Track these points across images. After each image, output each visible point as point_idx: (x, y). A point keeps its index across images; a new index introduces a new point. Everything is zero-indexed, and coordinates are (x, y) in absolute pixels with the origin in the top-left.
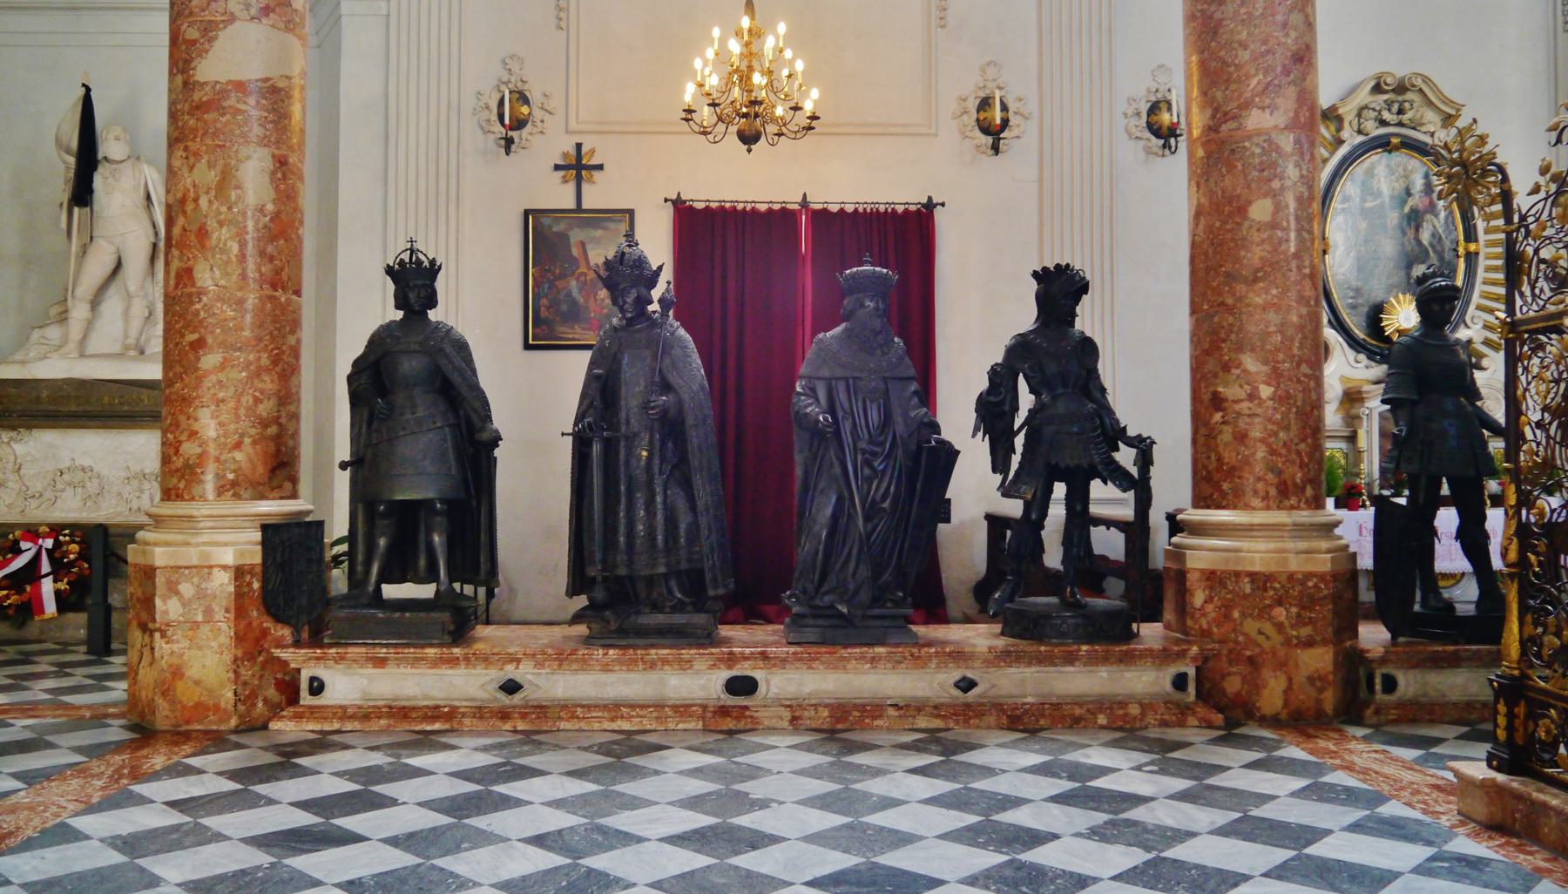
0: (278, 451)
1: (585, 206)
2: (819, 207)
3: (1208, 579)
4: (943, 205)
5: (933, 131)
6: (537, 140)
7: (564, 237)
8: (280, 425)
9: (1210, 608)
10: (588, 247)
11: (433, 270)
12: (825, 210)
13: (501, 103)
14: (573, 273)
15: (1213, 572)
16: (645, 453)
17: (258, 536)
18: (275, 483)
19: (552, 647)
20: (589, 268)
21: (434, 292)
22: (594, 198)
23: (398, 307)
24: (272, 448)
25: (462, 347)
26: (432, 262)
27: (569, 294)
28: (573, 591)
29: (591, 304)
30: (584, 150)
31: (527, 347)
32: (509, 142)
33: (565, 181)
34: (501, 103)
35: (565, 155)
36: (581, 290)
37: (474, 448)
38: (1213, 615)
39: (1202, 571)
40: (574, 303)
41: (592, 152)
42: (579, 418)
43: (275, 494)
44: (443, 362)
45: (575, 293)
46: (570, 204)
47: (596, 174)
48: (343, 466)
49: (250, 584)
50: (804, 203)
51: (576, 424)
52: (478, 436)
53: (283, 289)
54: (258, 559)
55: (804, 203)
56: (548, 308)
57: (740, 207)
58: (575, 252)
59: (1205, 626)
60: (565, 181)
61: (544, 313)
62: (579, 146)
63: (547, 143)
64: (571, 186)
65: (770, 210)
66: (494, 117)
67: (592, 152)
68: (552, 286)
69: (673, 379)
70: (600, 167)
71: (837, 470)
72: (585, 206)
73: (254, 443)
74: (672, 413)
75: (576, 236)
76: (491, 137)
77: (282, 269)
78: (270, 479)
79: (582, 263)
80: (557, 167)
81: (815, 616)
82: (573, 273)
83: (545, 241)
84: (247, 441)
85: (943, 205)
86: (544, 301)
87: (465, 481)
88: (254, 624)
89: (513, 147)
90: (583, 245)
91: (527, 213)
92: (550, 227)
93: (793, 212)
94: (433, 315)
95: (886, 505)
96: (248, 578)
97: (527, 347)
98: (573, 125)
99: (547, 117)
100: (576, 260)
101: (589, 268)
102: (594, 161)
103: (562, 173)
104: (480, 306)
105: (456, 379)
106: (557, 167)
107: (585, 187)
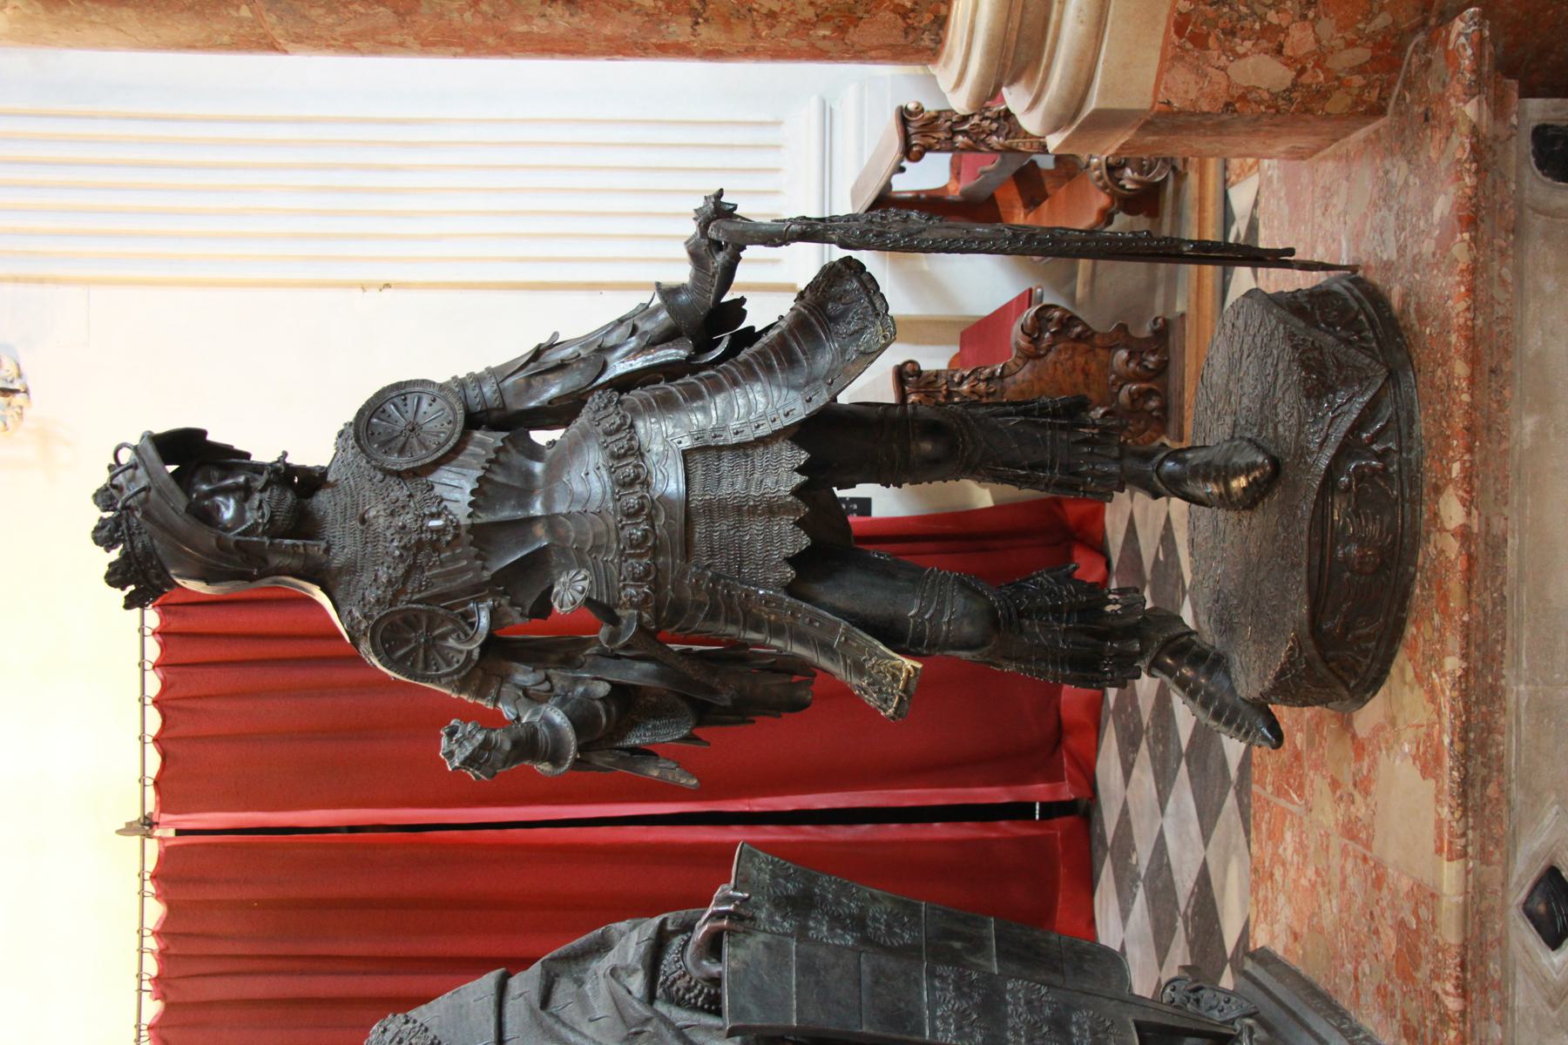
2: (151, 793)
3: (1200, 41)
9: (1300, 39)
15: (1180, 24)
38: (1327, 27)
39: (1169, 60)
55: (147, 825)
59: (1362, 54)
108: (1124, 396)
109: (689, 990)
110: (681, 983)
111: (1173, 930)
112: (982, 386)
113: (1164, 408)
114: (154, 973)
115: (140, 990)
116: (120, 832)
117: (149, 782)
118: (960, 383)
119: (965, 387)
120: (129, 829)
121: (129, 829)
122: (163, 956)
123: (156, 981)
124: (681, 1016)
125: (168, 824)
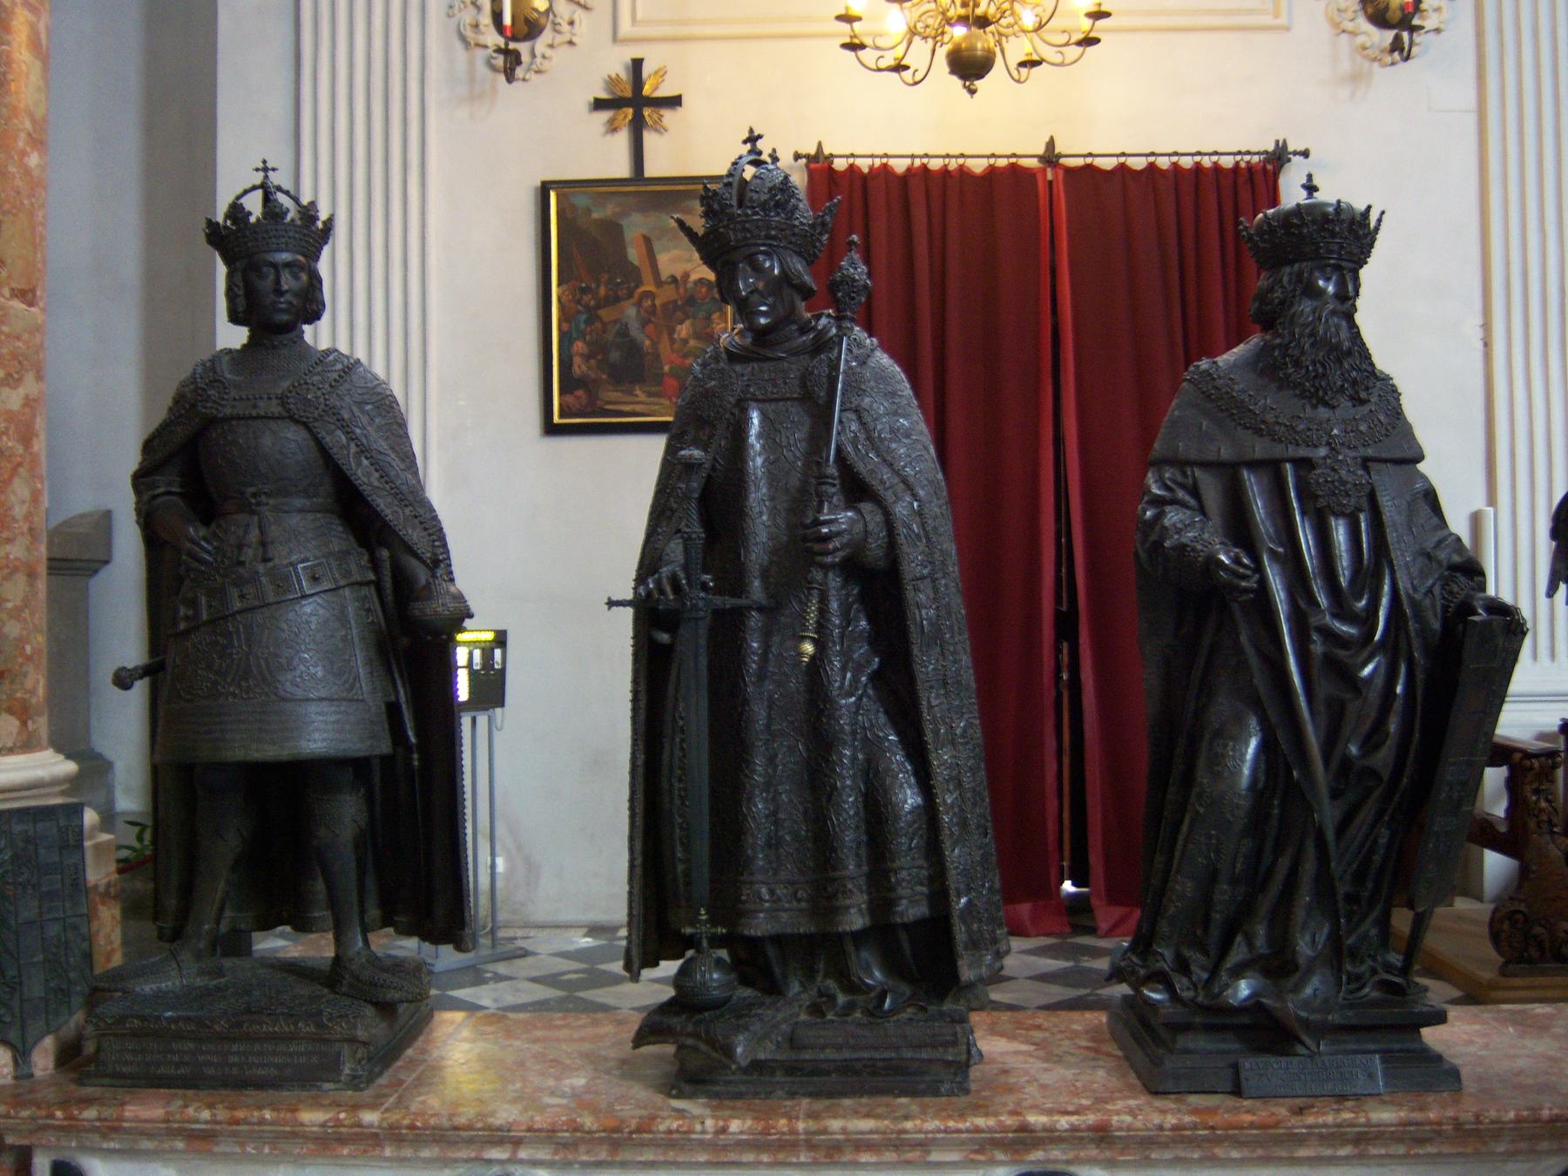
1: (651, 171)
2: (1080, 162)
4: (1306, 154)
5: (1282, 21)
6: (560, 56)
7: (613, 229)
10: (657, 246)
11: (312, 233)
12: (1089, 167)
14: (630, 296)
16: (808, 648)
19: (595, 1111)
20: (659, 283)
21: (315, 280)
22: (663, 159)
23: (235, 318)
26: (309, 213)
27: (624, 332)
28: (643, 955)
29: (665, 348)
30: (647, 70)
31: (551, 429)
32: (513, 59)
33: (612, 128)
35: (612, 82)
36: (645, 323)
37: (411, 628)
40: (633, 348)
41: (661, 73)
42: (649, 564)
44: (336, 439)
45: (635, 331)
46: (620, 167)
47: (668, 116)
48: (123, 680)
50: (1050, 157)
51: (640, 579)
52: (418, 609)
55: (1050, 157)
56: (587, 358)
57: (935, 164)
58: (634, 255)
60: (612, 128)
61: (580, 366)
62: (637, 64)
63: (580, 63)
64: (622, 139)
65: (992, 170)
66: (486, 19)
67: (661, 73)
68: (593, 317)
69: (868, 464)
70: (675, 102)
71: (1260, 681)
72: (651, 171)
74: (875, 548)
75: (635, 226)
76: (481, 55)
79: (647, 275)
80: (599, 105)
81: (1209, 1028)
82: (630, 296)
83: (584, 239)
85: (1306, 154)
86: (579, 346)
87: (393, 710)
89: (519, 72)
90: (647, 241)
91: (545, 188)
92: (589, 211)
93: (1028, 173)
94: (318, 336)
95: (1383, 758)
97: (551, 429)
98: (625, 27)
99: (579, 14)
100: (636, 271)
101: (659, 283)
102: (665, 91)
103: (605, 116)
104: (440, 324)
105: (363, 474)
106: (599, 105)
107: (649, 138)
108: (1538, 930)
109: (1451, 593)
110: (1456, 589)
111: (1075, 986)
112: (1545, 818)
113: (1530, 961)
114: (951, 168)
115: (913, 157)
116: (1052, 139)
117: (1089, 160)
118: (1547, 800)
119: (1543, 804)
120: (1051, 144)
121: (1051, 144)
122: (945, 171)
123: (924, 167)
124: (1437, 590)
125: (1056, 175)
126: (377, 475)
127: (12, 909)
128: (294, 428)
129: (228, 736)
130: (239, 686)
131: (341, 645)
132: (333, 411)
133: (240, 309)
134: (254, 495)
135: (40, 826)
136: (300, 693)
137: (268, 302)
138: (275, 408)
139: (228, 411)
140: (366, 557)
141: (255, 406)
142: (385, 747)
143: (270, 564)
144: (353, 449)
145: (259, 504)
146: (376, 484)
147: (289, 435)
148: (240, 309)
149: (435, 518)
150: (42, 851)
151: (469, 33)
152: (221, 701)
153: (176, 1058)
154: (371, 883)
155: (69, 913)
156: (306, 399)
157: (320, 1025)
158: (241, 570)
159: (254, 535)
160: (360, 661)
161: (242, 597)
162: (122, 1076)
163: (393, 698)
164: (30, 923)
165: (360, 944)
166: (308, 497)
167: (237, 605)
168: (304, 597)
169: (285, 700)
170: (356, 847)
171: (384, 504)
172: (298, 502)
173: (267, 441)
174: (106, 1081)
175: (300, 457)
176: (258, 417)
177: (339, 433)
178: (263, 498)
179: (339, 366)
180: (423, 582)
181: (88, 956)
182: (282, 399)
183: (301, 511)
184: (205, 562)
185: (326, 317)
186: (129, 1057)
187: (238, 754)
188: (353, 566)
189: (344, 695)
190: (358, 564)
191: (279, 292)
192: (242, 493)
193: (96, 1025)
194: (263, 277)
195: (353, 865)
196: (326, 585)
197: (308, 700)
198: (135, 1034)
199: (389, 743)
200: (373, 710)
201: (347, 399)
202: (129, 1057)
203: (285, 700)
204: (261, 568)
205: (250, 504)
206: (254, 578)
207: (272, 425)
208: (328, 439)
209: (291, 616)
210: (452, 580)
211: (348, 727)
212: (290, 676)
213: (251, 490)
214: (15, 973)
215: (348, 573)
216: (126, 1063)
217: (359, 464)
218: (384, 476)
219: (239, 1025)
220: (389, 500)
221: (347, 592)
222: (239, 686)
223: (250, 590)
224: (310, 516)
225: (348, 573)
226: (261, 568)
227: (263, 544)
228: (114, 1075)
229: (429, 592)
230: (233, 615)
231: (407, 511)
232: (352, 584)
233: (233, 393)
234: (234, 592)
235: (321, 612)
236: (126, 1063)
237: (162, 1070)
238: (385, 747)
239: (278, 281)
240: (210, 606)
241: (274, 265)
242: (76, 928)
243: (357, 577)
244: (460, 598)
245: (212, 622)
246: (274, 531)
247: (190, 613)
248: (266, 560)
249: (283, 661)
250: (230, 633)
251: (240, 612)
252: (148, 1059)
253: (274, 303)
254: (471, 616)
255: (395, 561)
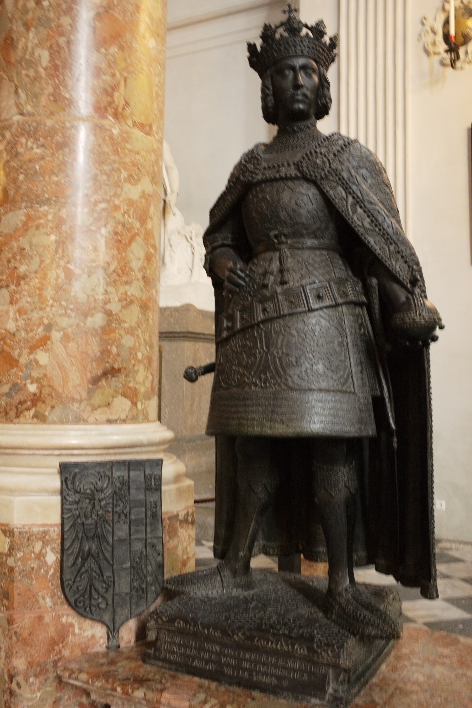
0: (105, 352)
8: (109, 314)
13: (447, 22)
17: (56, 483)
18: (98, 399)
24: (94, 348)
25: (376, 171)
34: (447, 22)
43: (100, 415)
44: (337, 193)
49: (40, 556)
53: (116, 115)
54: (55, 518)
66: (440, 38)
73: (66, 338)
76: (436, 59)
77: (114, 88)
78: (90, 393)
84: (56, 335)
88: (47, 619)
89: (458, 64)
96: (38, 546)
105: (358, 219)
126: (368, 220)
127: (110, 529)
128: (306, 185)
129: (250, 416)
130: (260, 379)
131: (338, 349)
132: (337, 173)
133: (270, 105)
134: (276, 237)
135: (132, 473)
136: (304, 385)
137: (289, 94)
138: (293, 172)
139: (259, 177)
140: (360, 285)
141: (278, 171)
142: (370, 430)
143: (286, 287)
144: (350, 200)
145: (280, 243)
146: (368, 226)
147: (303, 191)
148: (270, 105)
149: (413, 254)
150: (132, 491)
151: (431, 48)
152: (247, 389)
153: (207, 656)
154: (359, 532)
155: (149, 535)
156: (315, 163)
157: (310, 649)
158: (265, 292)
159: (275, 266)
160: (353, 361)
161: (264, 310)
162: (170, 662)
163: (379, 393)
164: (121, 541)
165: (348, 582)
166: (316, 237)
167: (261, 317)
168: (311, 310)
169: (292, 389)
170: (347, 507)
171: (373, 241)
172: (309, 242)
173: (286, 197)
174: (160, 663)
175: (310, 207)
176: (281, 179)
177: (340, 189)
178: (283, 239)
179: (341, 142)
180: (403, 299)
181: (161, 566)
182: (298, 166)
183: (312, 248)
184: (238, 285)
185: (333, 111)
186: (175, 649)
187: (256, 430)
188: (350, 290)
189: (340, 387)
190: (353, 290)
191: (297, 86)
192: (268, 236)
193: (156, 620)
194: (284, 77)
195: (344, 520)
196: (327, 302)
197: (311, 390)
198: (181, 632)
199: (374, 426)
200: (362, 401)
201: (346, 164)
202: (175, 649)
203: (292, 389)
204: (279, 289)
205: (274, 243)
206: (273, 297)
207: (290, 184)
208: (331, 193)
209: (301, 325)
210: (426, 297)
211: (341, 413)
212: (297, 371)
213: (272, 233)
214: (110, 574)
215: (345, 294)
216: (173, 653)
217: (355, 211)
218: (374, 221)
219: (251, 638)
220: (378, 238)
221: (344, 308)
222: (260, 379)
223: (270, 306)
224: (318, 252)
225: (345, 294)
226: (279, 289)
227: (281, 271)
228: (165, 660)
229: (408, 306)
230: (258, 324)
231: (392, 248)
232: (348, 303)
233: (264, 164)
234: (259, 308)
235: (323, 321)
236: (173, 653)
237: (196, 663)
238: (370, 430)
239: (296, 78)
240: (242, 318)
241: (293, 68)
242: (153, 546)
243: (352, 297)
244: (434, 312)
245: (243, 330)
246: (290, 263)
247: (230, 324)
248: (283, 283)
249: (293, 359)
250: (255, 338)
251: (263, 322)
252: (188, 652)
253: (293, 96)
254: (442, 327)
255: (381, 287)
